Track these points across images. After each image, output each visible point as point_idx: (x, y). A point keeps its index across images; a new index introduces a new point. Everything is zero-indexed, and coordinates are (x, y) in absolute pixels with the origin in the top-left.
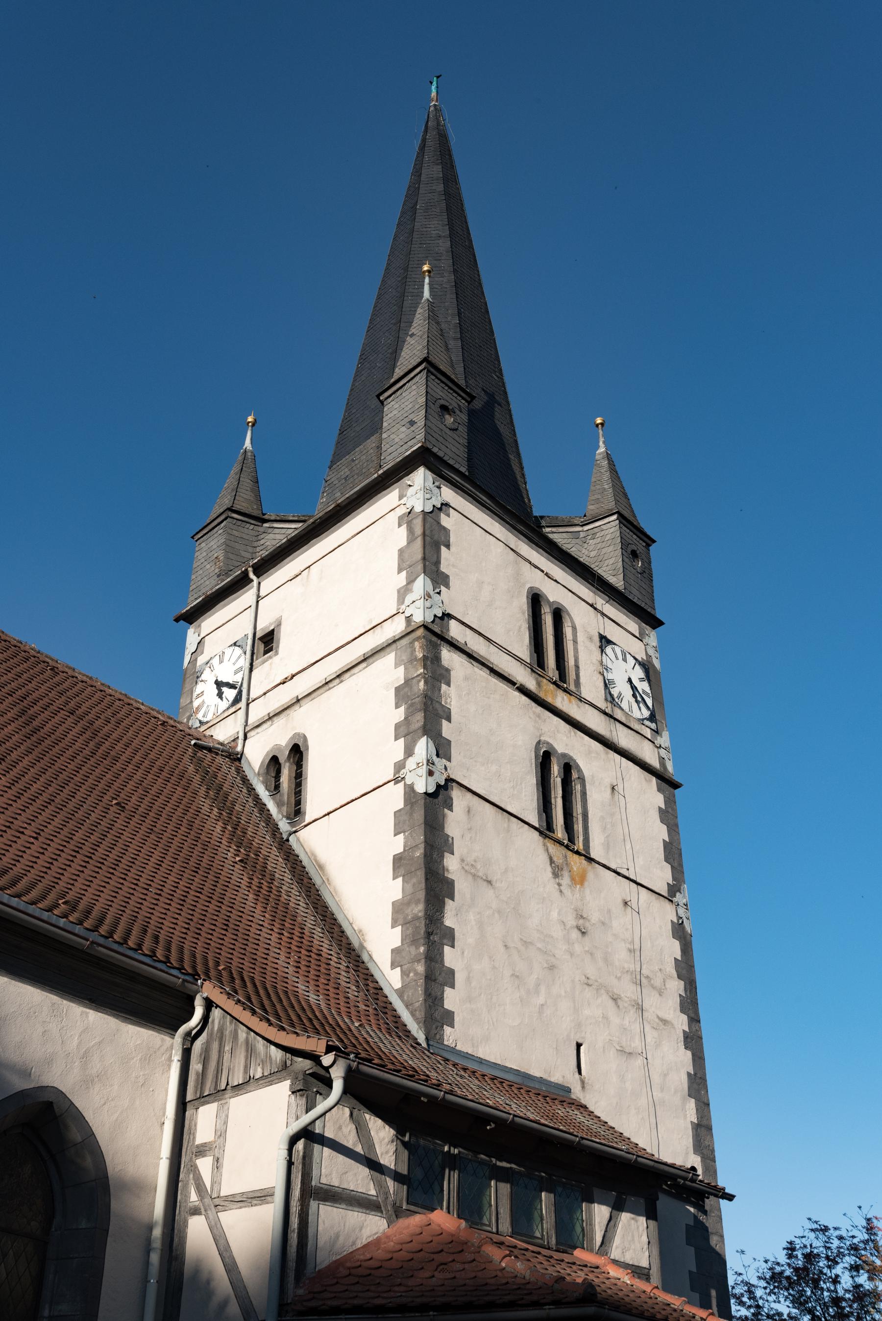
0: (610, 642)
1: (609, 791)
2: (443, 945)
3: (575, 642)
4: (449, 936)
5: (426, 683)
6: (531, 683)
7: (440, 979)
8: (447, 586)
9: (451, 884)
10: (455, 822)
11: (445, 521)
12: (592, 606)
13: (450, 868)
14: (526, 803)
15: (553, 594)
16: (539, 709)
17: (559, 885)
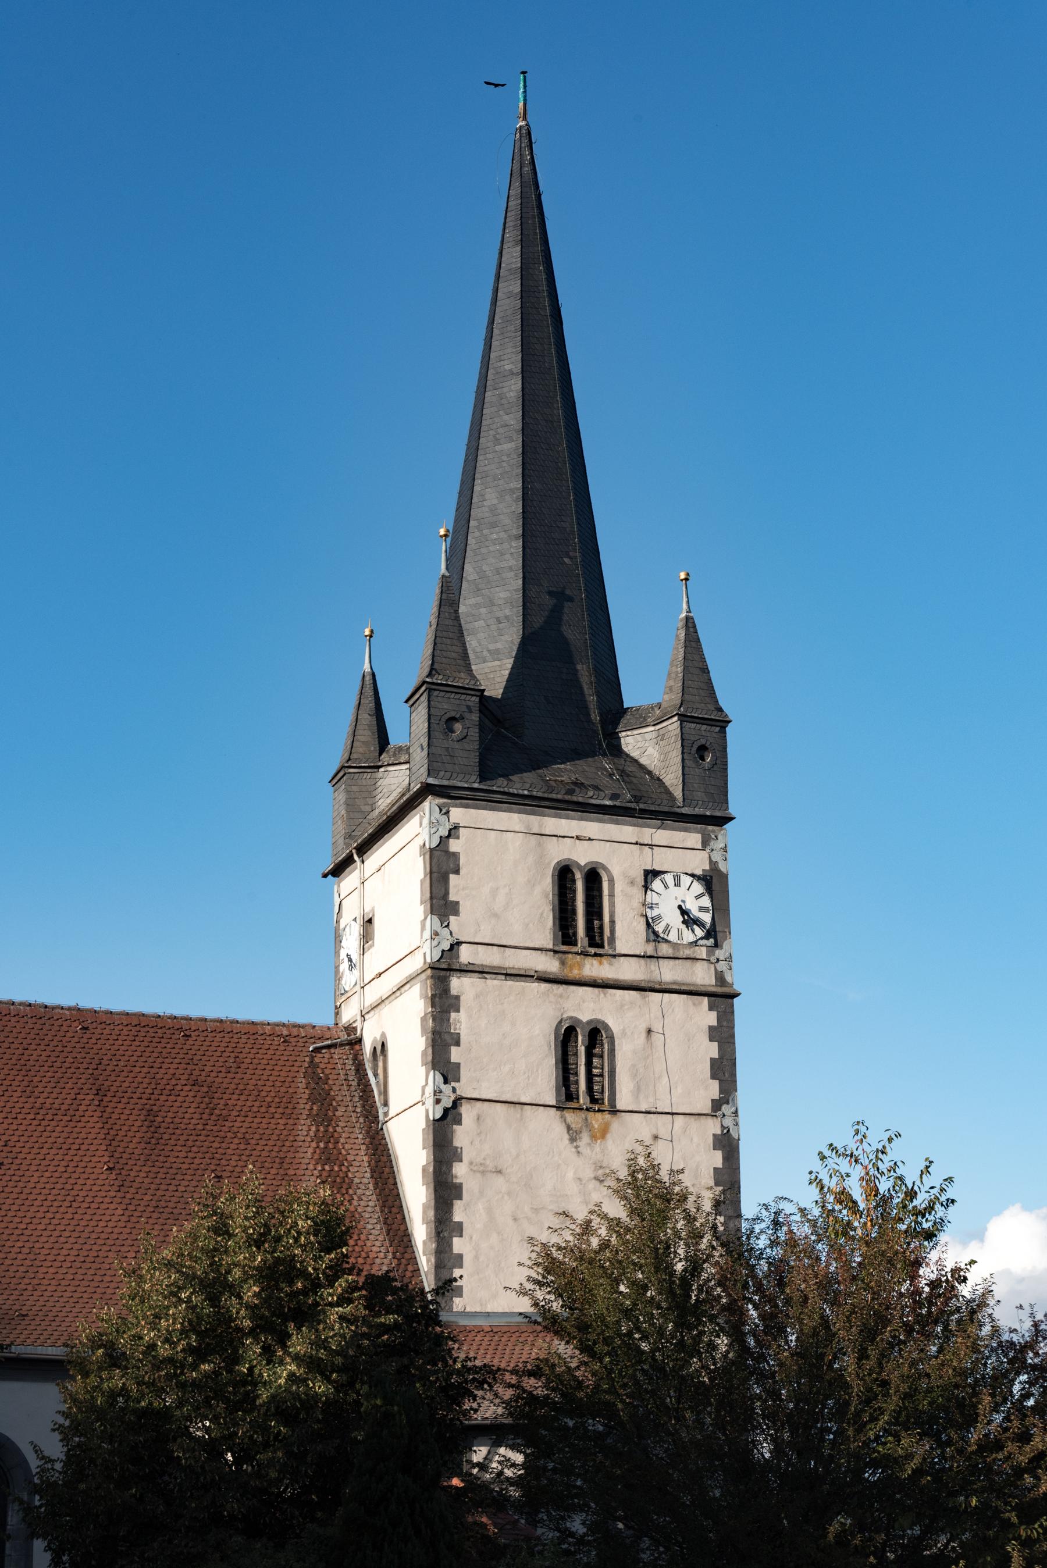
1: (644, 1035)
2: (452, 1238)
3: (612, 895)
4: (459, 1229)
5: (434, 1020)
6: (550, 965)
7: (450, 1264)
8: (456, 913)
9: (459, 1187)
10: (462, 1136)
11: (454, 846)
12: (636, 843)
13: (459, 1174)
14: (544, 1084)
15: (583, 856)
16: (561, 989)
17: (577, 1147)
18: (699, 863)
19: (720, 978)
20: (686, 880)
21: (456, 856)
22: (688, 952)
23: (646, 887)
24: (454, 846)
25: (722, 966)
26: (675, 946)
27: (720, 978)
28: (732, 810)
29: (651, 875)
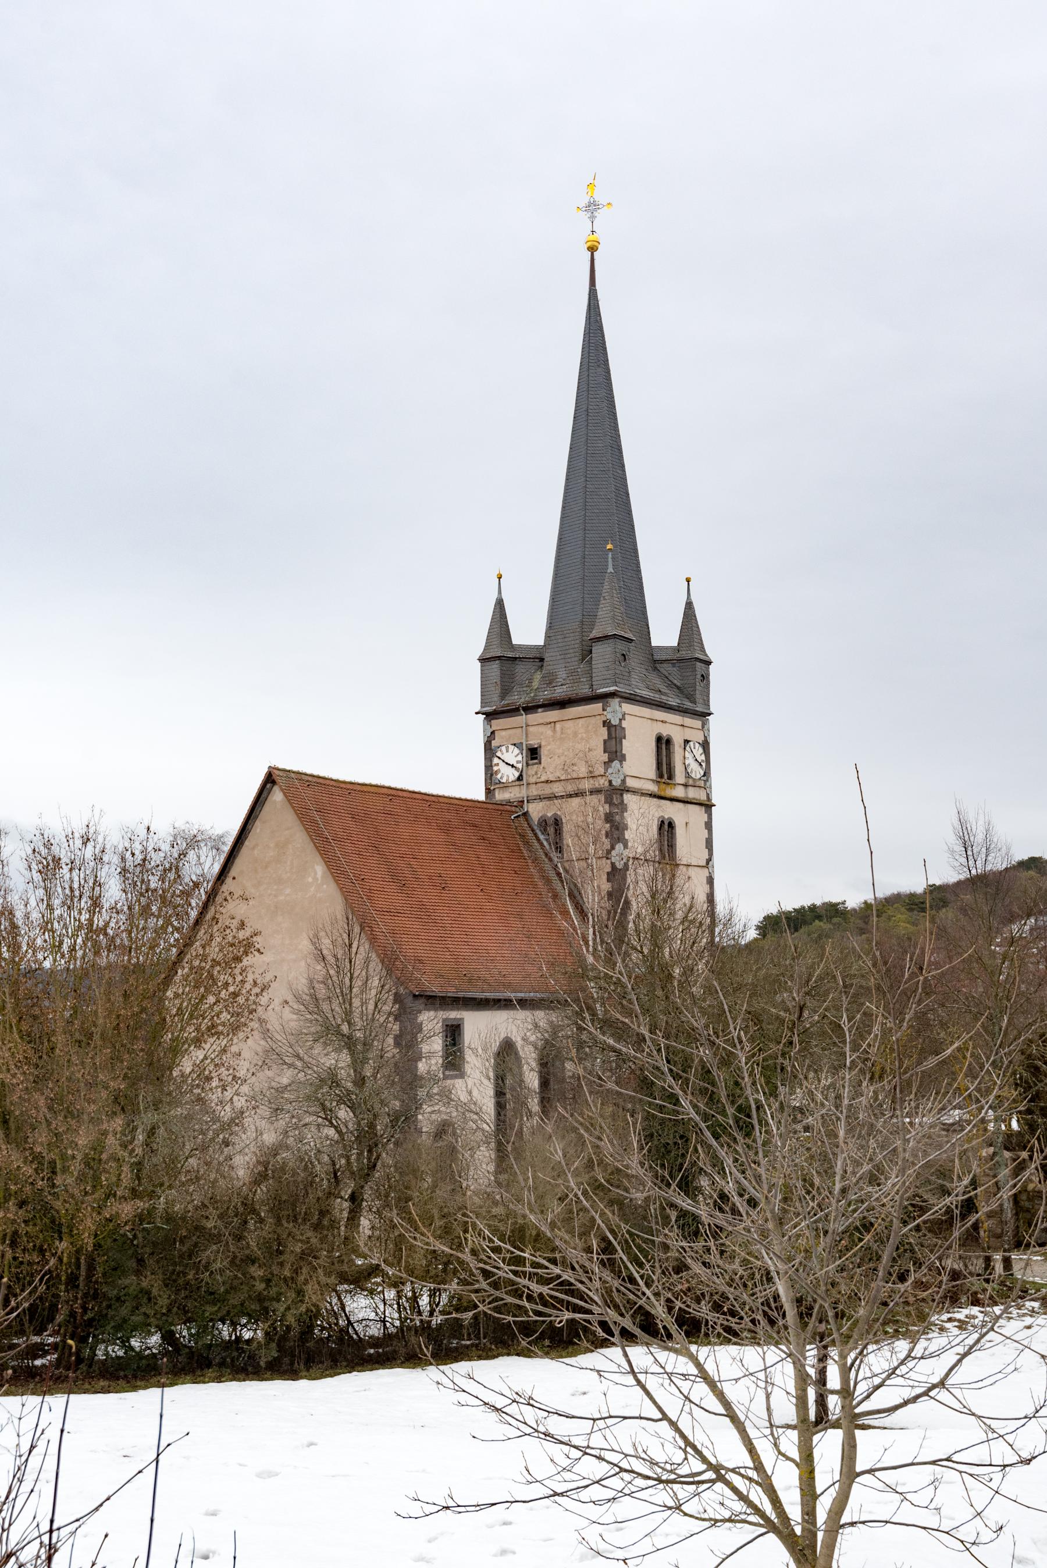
11: (624, 724)
15: (665, 731)
20: (697, 745)
27: (709, 799)
28: (712, 710)
29: (687, 742)
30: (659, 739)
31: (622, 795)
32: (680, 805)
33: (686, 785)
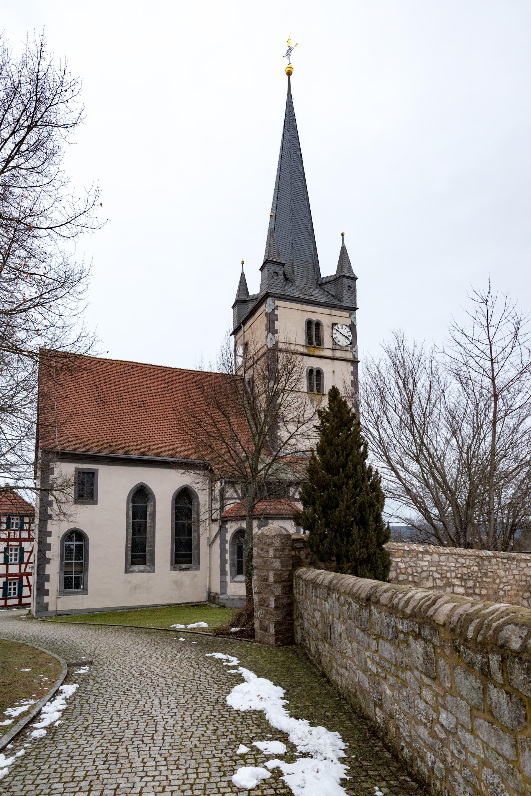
0: (336, 324)
8: (277, 333)
11: (276, 312)
15: (314, 318)
18: (348, 322)
19: (354, 356)
20: (344, 327)
21: (277, 315)
22: (345, 349)
23: (332, 328)
24: (276, 312)
25: (354, 353)
26: (341, 346)
27: (354, 356)
28: (358, 306)
29: (334, 324)
30: (309, 323)
31: (274, 353)
32: (329, 361)
33: (333, 349)
